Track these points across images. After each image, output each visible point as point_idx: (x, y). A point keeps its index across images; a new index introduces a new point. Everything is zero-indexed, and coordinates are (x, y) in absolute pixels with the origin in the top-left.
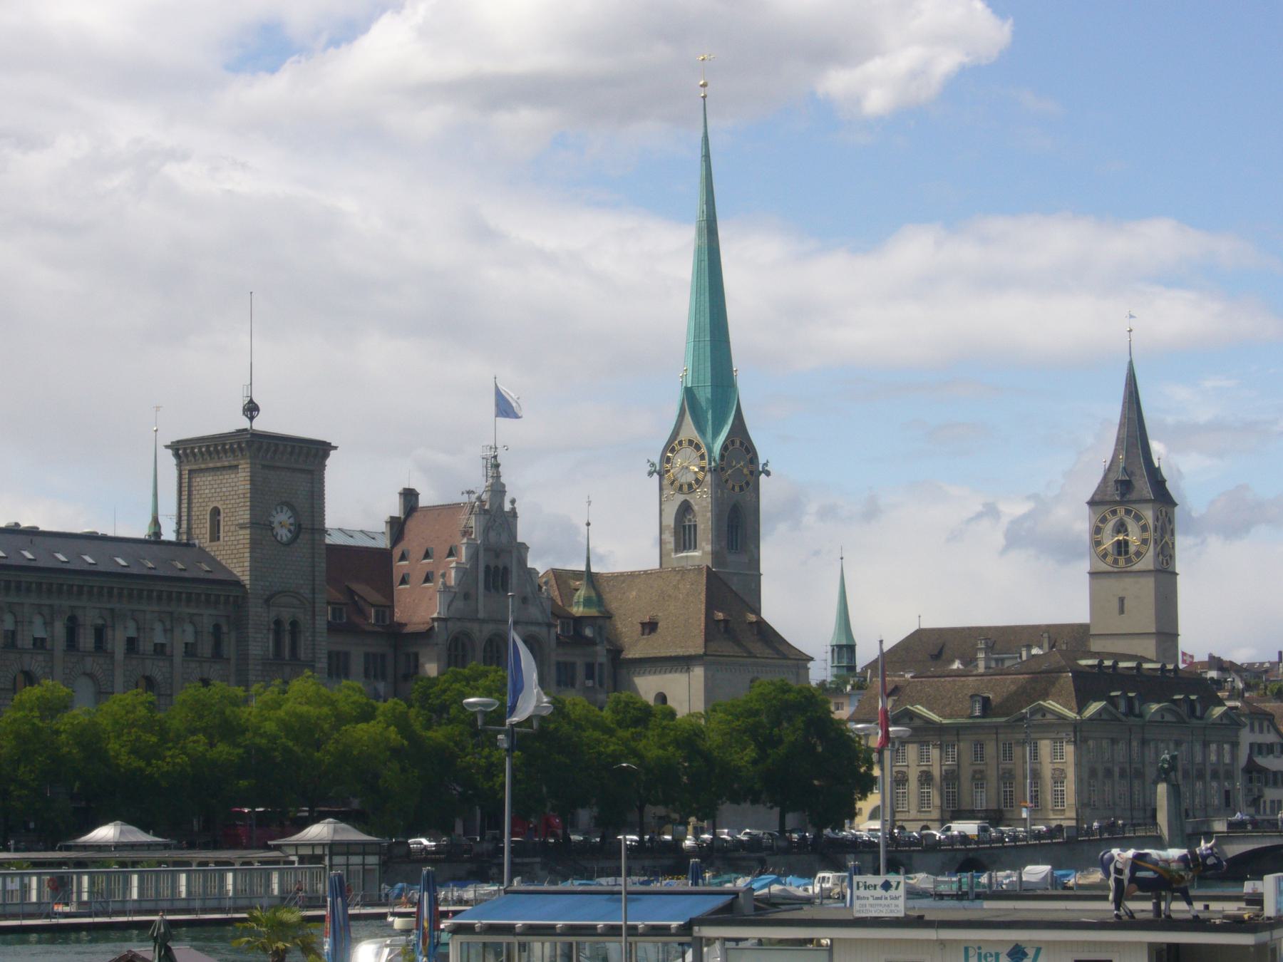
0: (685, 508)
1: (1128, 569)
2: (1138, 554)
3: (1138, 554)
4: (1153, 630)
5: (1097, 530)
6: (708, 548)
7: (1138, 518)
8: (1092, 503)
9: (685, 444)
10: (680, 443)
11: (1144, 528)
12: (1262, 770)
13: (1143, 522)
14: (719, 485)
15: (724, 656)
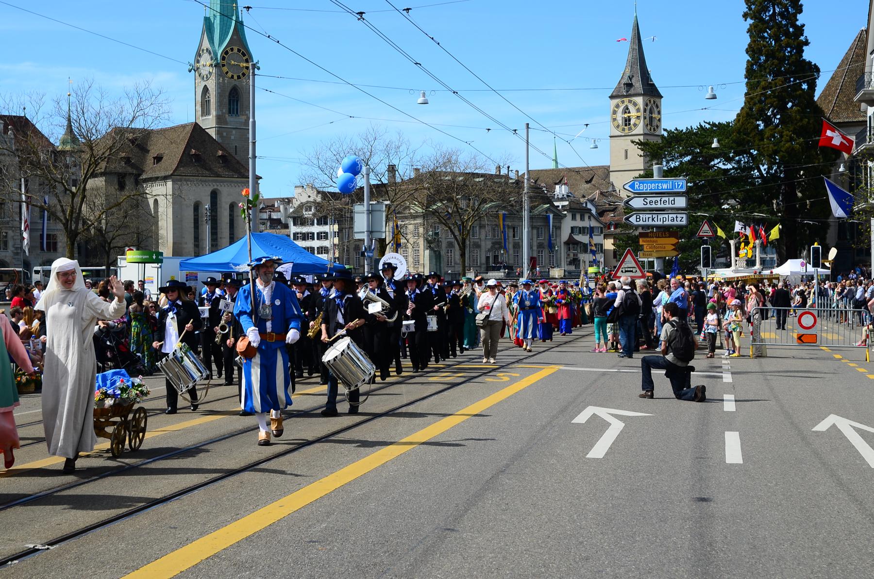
0: (206, 90)
1: (630, 134)
2: (635, 125)
3: (635, 125)
4: (642, 168)
5: (615, 112)
6: (214, 113)
7: (635, 104)
8: (612, 97)
9: (205, 51)
10: (203, 50)
11: (638, 110)
12: (577, 243)
13: (637, 107)
14: (220, 75)
15: (188, 176)
